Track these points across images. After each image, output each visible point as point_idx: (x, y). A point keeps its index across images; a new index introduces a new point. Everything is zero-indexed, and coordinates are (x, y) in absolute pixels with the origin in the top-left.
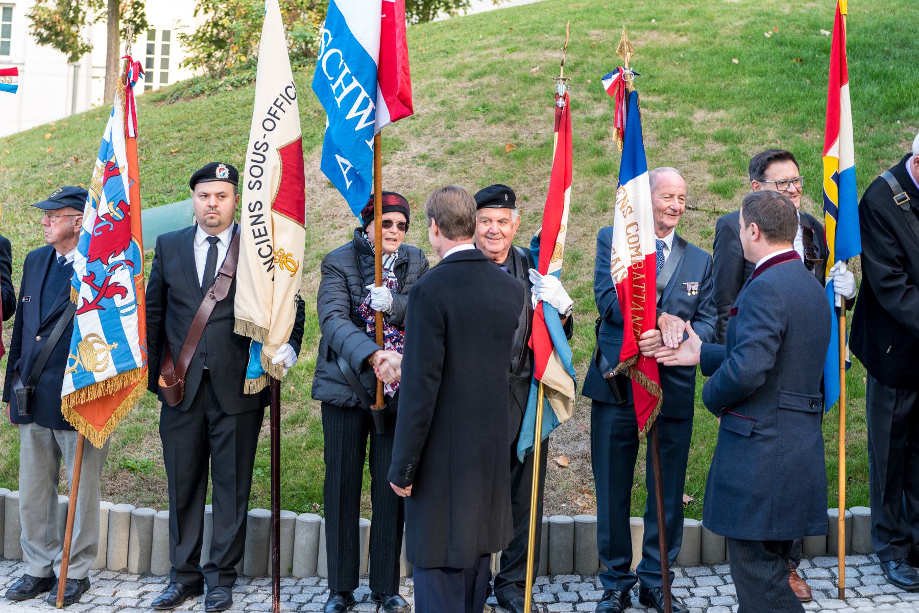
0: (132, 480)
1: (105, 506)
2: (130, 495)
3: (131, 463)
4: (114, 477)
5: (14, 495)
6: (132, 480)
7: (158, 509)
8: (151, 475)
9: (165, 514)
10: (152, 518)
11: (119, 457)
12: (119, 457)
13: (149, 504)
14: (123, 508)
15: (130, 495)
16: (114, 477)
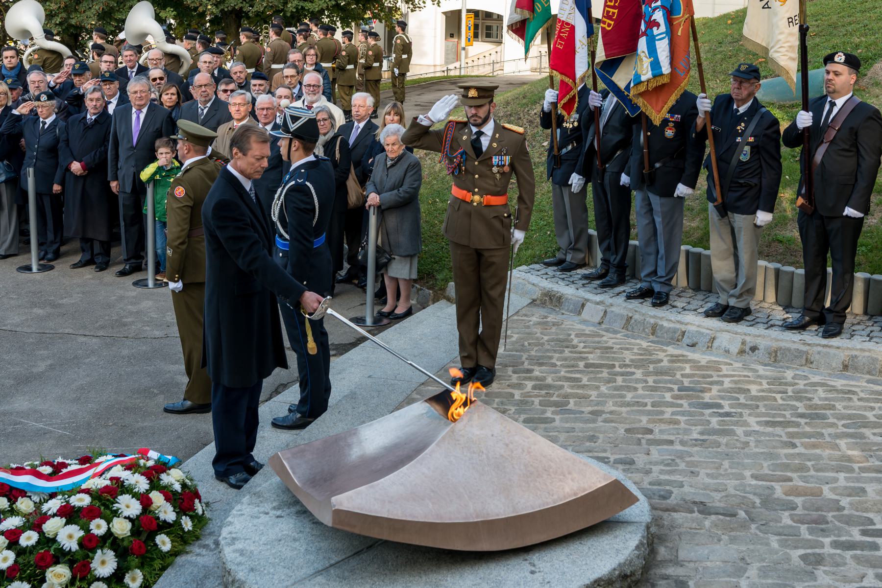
0: (781, 248)
1: (762, 263)
2: (779, 257)
3: (780, 237)
4: (769, 246)
5: (707, 252)
6: (781, 248)
7: (797, 268)
8: (792, 246)
9: (802, 271)
10: (793, 273)
11: (773, 233)
12: (773, 233)
13: (791, 264)
14: (772, 266)
15: (779, 257)
16: (769, 246)
